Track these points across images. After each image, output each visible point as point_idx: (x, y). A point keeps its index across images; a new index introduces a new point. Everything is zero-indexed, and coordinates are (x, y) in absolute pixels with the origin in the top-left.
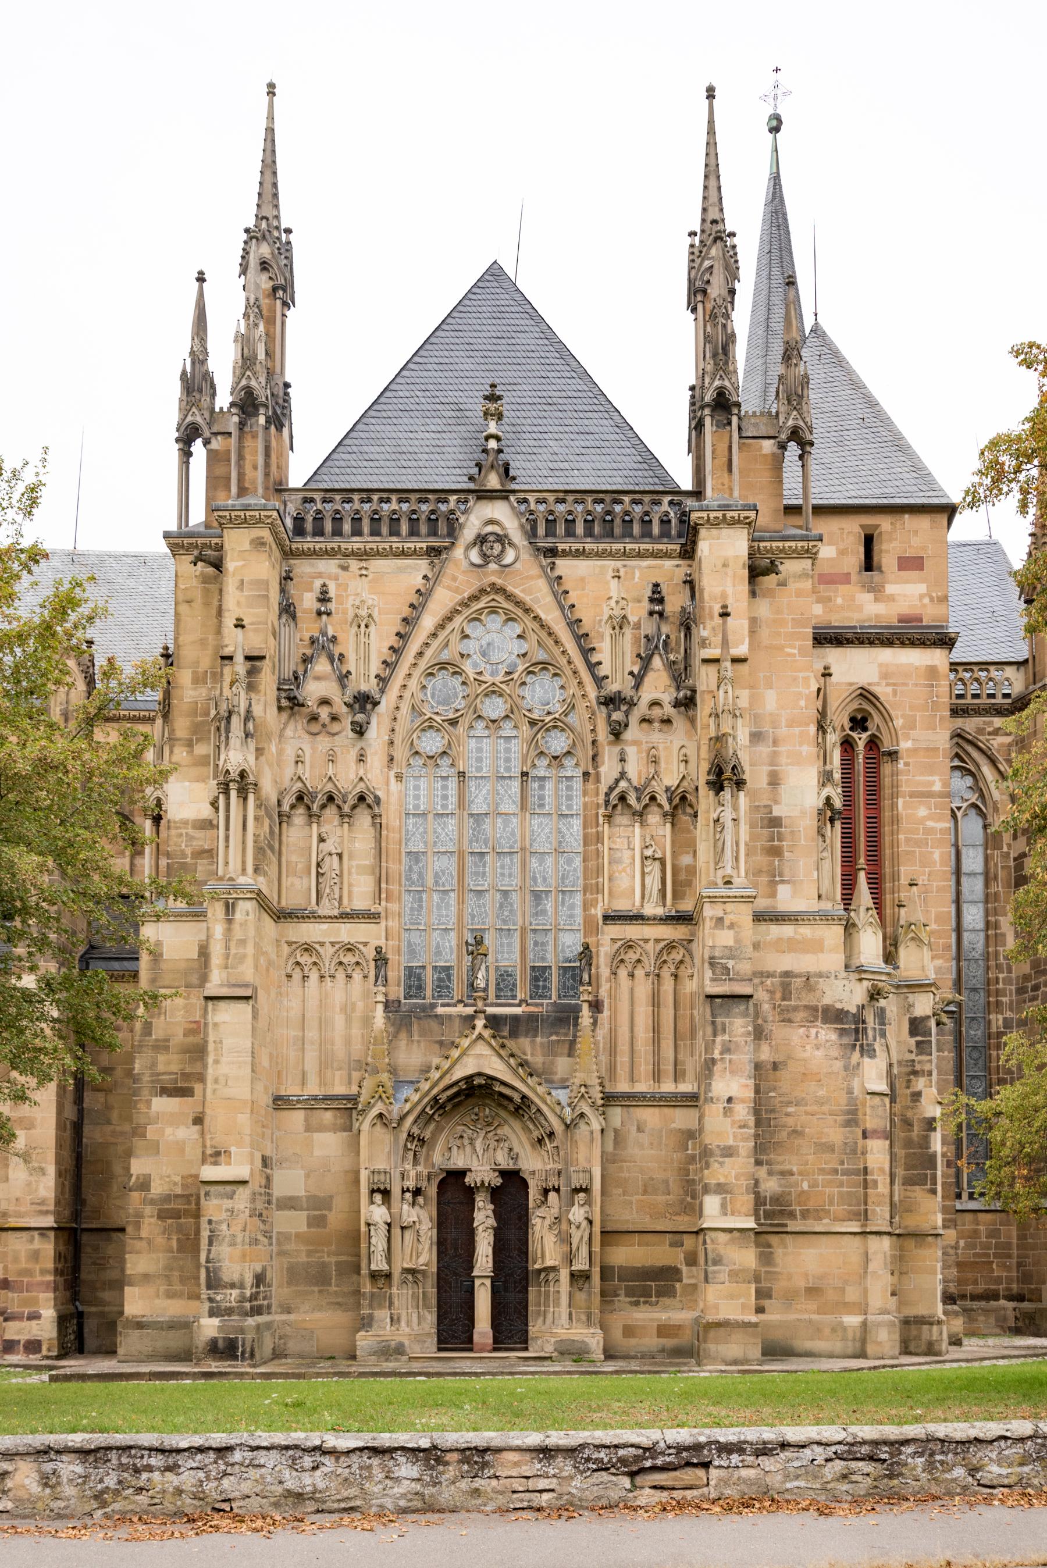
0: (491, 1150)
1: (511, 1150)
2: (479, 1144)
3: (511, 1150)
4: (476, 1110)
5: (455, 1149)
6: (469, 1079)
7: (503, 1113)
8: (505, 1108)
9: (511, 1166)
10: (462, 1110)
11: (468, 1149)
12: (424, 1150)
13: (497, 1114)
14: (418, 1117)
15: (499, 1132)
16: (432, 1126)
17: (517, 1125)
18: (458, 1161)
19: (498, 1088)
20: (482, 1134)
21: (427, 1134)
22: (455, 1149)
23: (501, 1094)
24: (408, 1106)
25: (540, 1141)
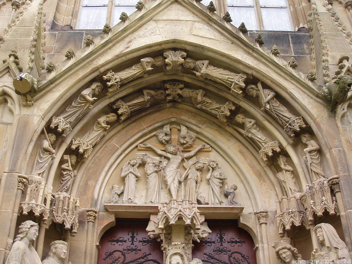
0: (191, 183)
1: (223, 181)
2: (172, 172)
3: (223, 181)
4: (167, 129)
5: (131, 179)
6: (157, 52)
7: (209, 132)
8: (211, 119)
9: (226, 204)
10: (145, 125)
11: (154, 180)
12: (81, 175)
13: (199, 136)
14: (68, 103)
15: (204, 160)
16: (94, 135)
17: (232, 147)
18: (137, 197)
19: (205, 69)
20: (176, 160)
21: (85, 143)
22: (131, 179)
23: (208, 80)
24: (53, 75)
25: (274, 161)
